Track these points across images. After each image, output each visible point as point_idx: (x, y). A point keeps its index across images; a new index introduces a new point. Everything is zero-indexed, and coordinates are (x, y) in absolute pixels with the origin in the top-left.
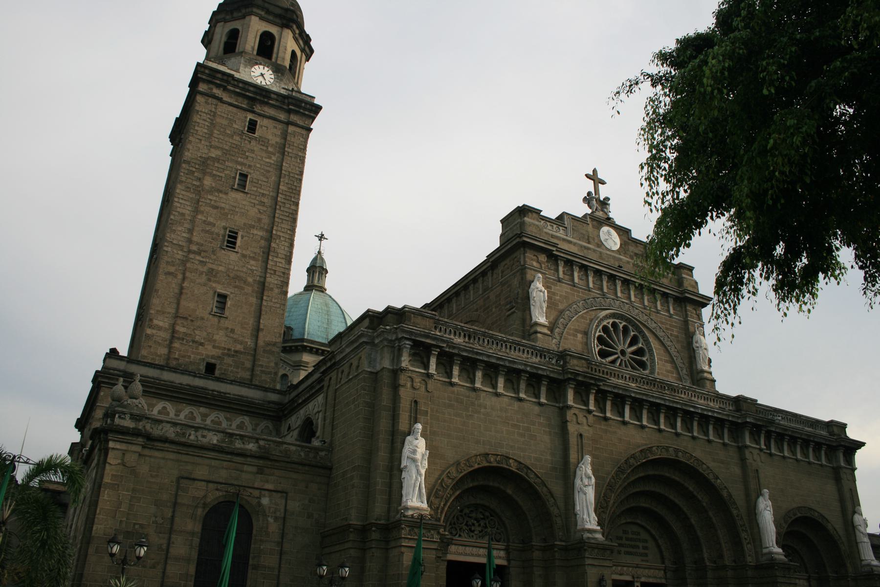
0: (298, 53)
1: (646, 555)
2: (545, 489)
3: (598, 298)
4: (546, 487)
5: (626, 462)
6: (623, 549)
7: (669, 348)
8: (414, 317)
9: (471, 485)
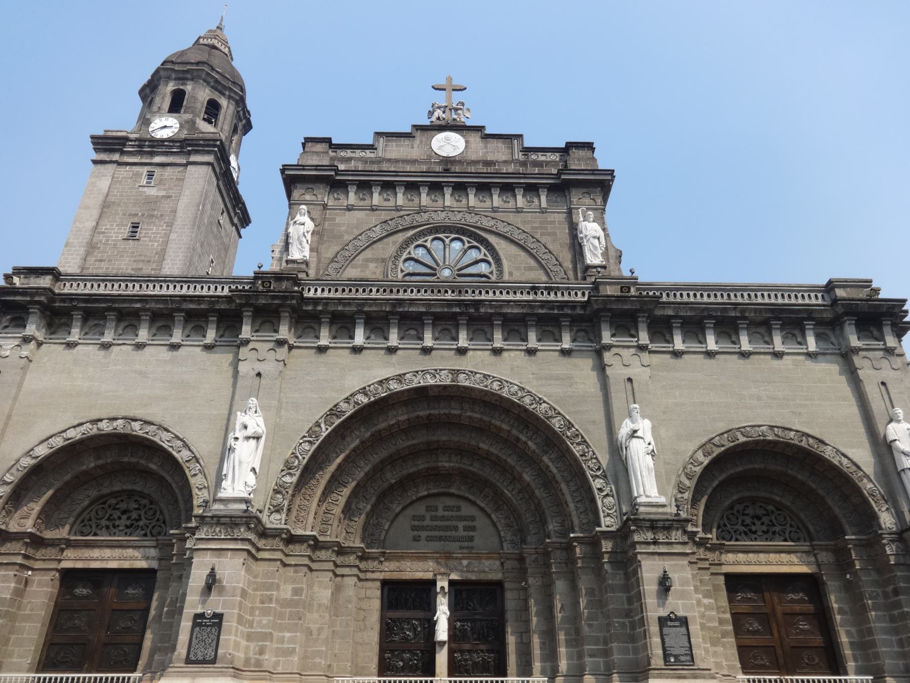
0: (223, 102)
1: (471, 539)
2: (188, 453)
3: (408, 215)
4: (190, 450)
5: (347, 400)
6: (424, 534)
7: (534, 252)
8: (25, 278)
9: (93, 465)
